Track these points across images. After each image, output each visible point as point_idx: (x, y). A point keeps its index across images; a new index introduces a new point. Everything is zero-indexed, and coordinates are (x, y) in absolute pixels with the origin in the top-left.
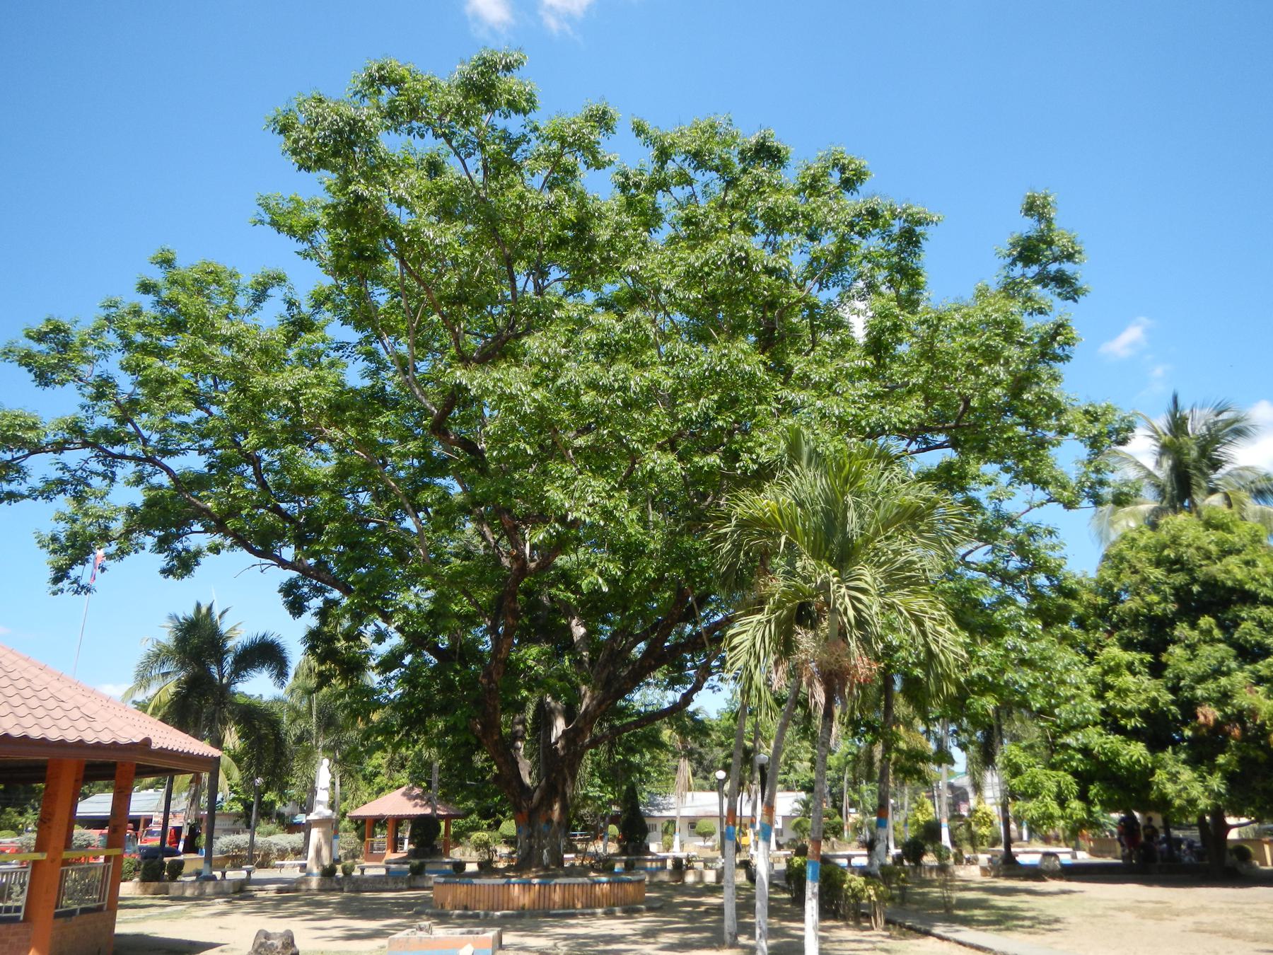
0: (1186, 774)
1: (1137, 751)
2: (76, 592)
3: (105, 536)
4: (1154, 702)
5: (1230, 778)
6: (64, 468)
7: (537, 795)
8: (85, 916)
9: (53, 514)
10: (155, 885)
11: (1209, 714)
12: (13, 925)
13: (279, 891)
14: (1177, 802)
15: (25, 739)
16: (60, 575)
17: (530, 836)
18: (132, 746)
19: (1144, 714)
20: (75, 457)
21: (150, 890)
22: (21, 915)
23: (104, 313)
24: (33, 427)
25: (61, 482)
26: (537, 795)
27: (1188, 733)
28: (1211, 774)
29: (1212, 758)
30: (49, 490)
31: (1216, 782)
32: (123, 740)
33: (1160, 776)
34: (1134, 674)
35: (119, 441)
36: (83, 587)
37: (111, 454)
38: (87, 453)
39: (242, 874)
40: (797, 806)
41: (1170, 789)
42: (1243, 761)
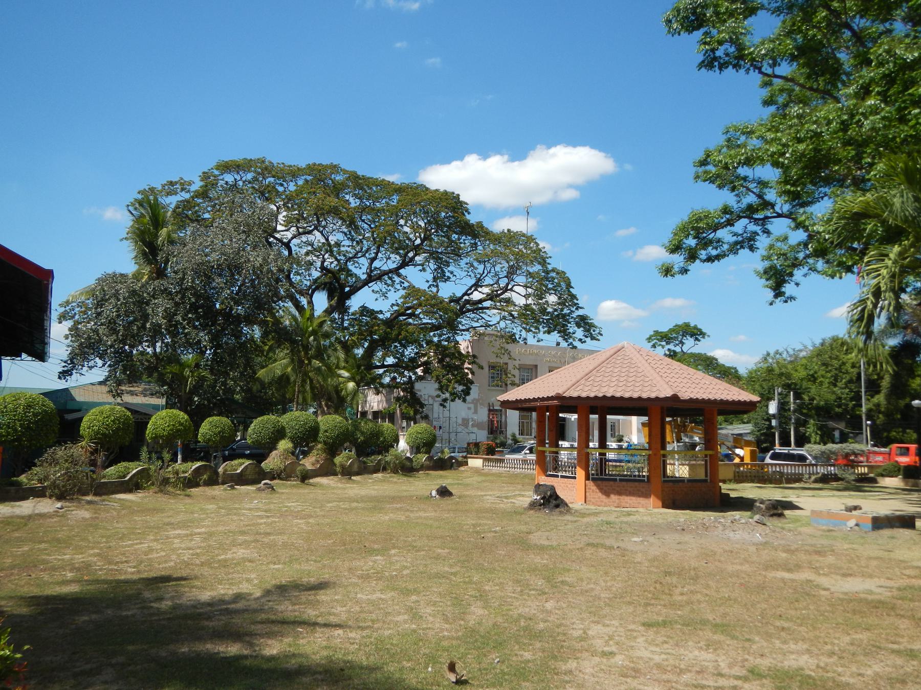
2: (786, 302)
3: (796, 264)
6: (735, 234)
8: (690, 484)
9: (760, 258)
10: (911, 480)
12: (641, 484)
15: (640, 398)
16: (778, 293)
18: (666, 399)
20: (741, 225)
21: (910, 484)
22: (646, 479)
23: (725, 137)
24: (706, 217)
25: (736, 243)
30: (735, 248)
32: (662, 396)
35: (757, 211)
36: (788, 298)
37: (756, 219)
38: (744, 221)
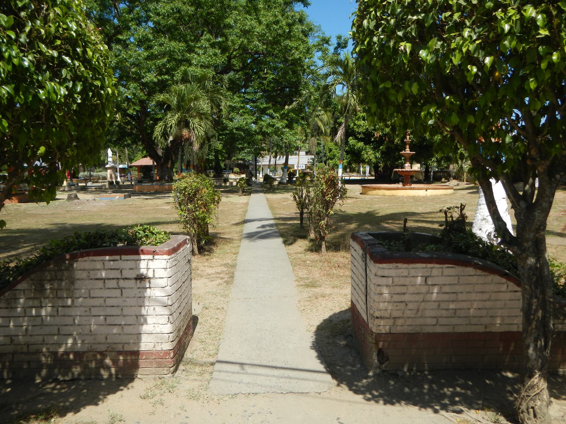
0: (371, 152)
1: (361, 144)
4: (367, 129)
5: (383, 153)
7: (162, 160)
11: (377, 134)
13: (96, 189)
14: (366, 160)
17: (162, 172)
19: (364, 133)
26: (162, 160)
27: (373, 139)
28: (378, 152)
29: (379, 147)
31: (378, 155)
33: (363, 152)
34: (364, 120)
39: (84, 184)
40: (311, 161)
41: (365, 156)
42: (388, 148)
